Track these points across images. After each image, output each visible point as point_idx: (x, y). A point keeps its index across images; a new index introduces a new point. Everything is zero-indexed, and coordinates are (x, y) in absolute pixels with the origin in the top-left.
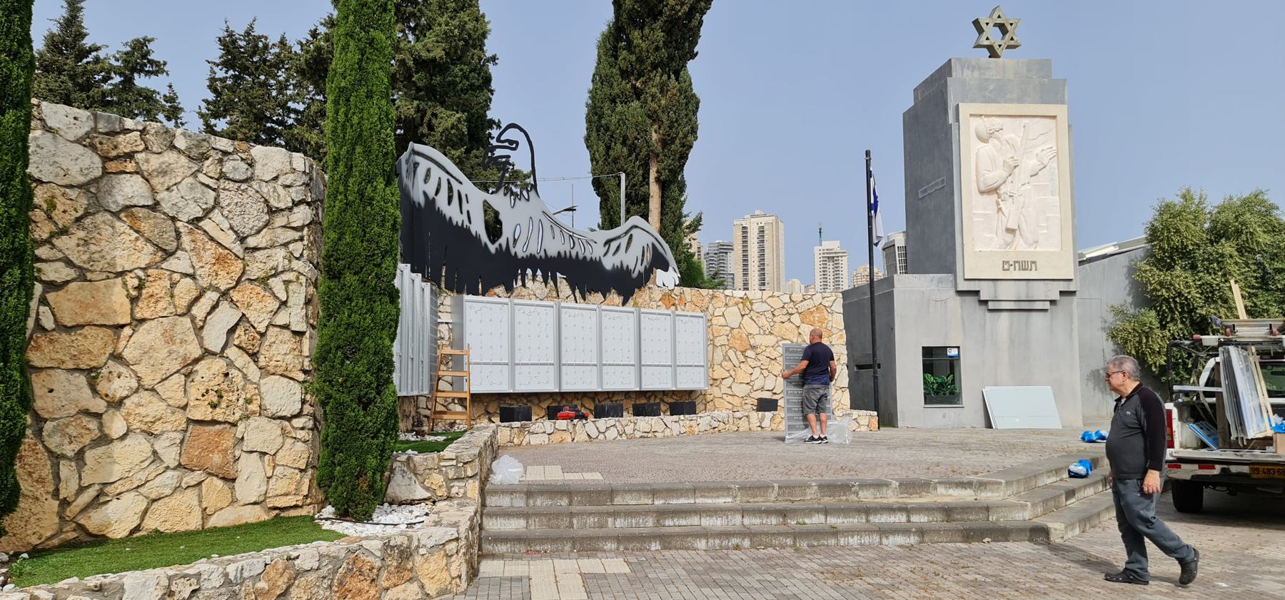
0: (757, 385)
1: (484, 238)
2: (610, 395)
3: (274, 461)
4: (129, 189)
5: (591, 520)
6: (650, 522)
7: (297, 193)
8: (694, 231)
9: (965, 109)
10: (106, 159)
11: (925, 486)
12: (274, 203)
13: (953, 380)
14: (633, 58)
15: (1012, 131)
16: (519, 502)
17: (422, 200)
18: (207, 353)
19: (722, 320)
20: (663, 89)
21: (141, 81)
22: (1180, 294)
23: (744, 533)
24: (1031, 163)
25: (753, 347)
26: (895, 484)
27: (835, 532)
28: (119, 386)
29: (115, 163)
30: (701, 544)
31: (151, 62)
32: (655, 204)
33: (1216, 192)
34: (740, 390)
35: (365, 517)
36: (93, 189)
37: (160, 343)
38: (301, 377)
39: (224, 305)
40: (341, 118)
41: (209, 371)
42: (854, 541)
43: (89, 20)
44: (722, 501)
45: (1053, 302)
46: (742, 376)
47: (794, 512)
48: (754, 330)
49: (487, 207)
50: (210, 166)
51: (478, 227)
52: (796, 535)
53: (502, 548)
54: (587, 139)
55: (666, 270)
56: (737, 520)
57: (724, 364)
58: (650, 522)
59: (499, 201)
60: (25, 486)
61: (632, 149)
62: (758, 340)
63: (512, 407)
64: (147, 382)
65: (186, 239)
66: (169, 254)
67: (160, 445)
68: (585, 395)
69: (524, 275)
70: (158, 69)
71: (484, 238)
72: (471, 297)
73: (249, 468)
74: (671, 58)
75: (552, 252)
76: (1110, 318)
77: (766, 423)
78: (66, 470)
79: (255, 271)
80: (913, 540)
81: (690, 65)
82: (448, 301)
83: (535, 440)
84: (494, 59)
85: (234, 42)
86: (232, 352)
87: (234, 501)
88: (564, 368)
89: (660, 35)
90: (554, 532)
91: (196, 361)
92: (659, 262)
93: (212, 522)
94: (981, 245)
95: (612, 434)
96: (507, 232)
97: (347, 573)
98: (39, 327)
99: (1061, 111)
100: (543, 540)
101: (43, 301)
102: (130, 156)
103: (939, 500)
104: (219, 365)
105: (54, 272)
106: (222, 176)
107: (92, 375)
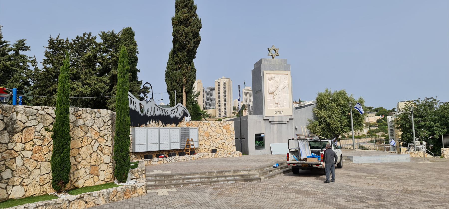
1: (140, 112)
2: (172, 150)
3: (106, 172)
4: (80, 122)
6: (181, 181)
7: (109, 118)
9: (265, 72)
10: (76, 117)
11: (238, 171)
12: (105, 121)
13: (263, 143)
15: (277, 78)
16: (153, 178)
20: (187, 67)
21: (21, 53)
22: (323, 117)
23: (200, 183)
24: (282, 86)
25: (211, 136)
27: (218, 181)
28: (80, 159)
29: (78, 117)
30: (192, 185)
31: (25, 47)
33: (334, 89)
34: (207, 147)
35: (125, 182)
38: (110, 155)
39: (97, 142)
40: (119, 105)
41: (94, 155)
42: (222, 183)
45: (287, 121)
46: (208, 143)
47: (211, 178)
48: (211, 131)
49: (140, 104)
51: (138, 110)
52: (211, 182)
53: (151, 188)
54: (166, 80)
55: (187, 116)
56: (199, 180)
58: (181, 181)
61: (178, 83)
62: (212, 134)
63: (148, 155)
64: (84, 158)
65: (90, 130)
66: (87, 133)
68: (166, 151)
70: (27, 49)
71: (140, 112)
73: (102, 173)
74: (189, 59)
75: (157, 114)
76: (308, 122)
77: (213, 156)
79: (102, 135)
80: (234, 182)
81: (194, 60)
83: (154, 163)
84: (138, 52)
87: (99, 180)
89: (185, 54)
92: (185, 115)
93: (95, 184)
94: (269, 107)
95: (173, 161)
96: (146, 110)
97: (126, 192)
99: (289, 72)
102: (80, 115)
104: (96, 154)
106: (96, 117)
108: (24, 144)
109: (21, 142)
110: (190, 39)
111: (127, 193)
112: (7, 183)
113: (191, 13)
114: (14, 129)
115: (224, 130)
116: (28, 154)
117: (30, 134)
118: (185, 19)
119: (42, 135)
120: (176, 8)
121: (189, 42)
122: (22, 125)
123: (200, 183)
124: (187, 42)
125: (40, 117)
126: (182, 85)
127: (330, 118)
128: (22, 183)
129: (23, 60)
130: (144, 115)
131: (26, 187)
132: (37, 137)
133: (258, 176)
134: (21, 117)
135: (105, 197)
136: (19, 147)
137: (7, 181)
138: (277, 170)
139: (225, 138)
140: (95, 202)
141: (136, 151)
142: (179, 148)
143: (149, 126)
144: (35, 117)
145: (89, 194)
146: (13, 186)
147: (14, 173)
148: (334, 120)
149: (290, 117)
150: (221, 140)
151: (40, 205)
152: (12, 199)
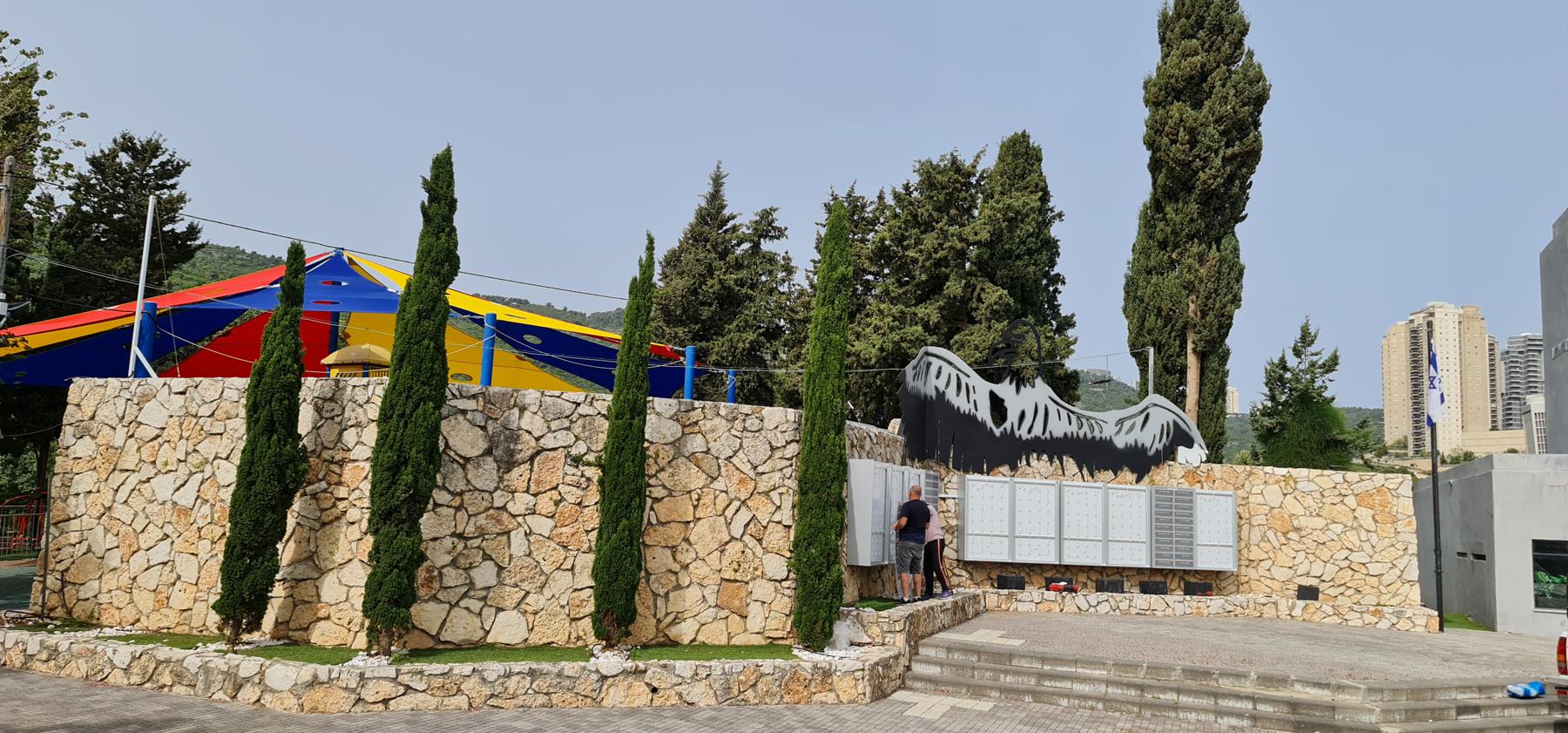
0: (1302, 569)
1: (990, 424)
3: (770, 608)
4: (696, 444)
5: (988, 674)
6: (1033, 681)
7: (789, 436)
8: (1327, 372)
10: (684, 426)
11: (1283, 681)
14: (1169, 230)
16: (942, 655)
17: (934, 394)
19: (1260, 499)
20: (1201, 259)
21: (766, 246)
23: (1097, 699)
25: (1297, 529)
26: (1253, 675)
27: (1175, 707)
28: (686, 557)
29: (689, 427)
30: (1064, 702)
34: (1281, 574)
35: (820, 649)
36: (677, 444)
39: (743, 509)
41: (734, 549)
42: (1192, 716)
43: (728, 193)
44: (1097, 673)
46: (1283, 558)
47: (1150, 688)
48: (1299, 510)
50: (738, 424)
51: (984, 414)
52: (1142, 705)
53: (919, 685)
54: (1125, 310)
56: (1102, 688)
57: (1262, 544)
58: (1033, 681)
59: (1005, 390)
60: (640, 610)
61: (1168, 320)
62: (1302, 522)
63: (1010, 576)
64: (701, 555)
67: (707, 592)
68: (1092, 568)
70: (780, 233)
71: (990, 424)
72: (977, 476)
73: (755, 610)
74: (1209, 227)
77: (1297, 612)
78: (660, 602)
79: (761, 488)
80: (1246, 723)
81: (1239, 228)
82: (955, 479)
83: (1022, 607)
86: (747, 538)
88: (1066, 543)
89: (1194, 208)
90: (961, 680)
96: (1012, 417)
97: (788, 681)
98: (650, 523)
100: (947, 683)
101: (652, 509)
102: (696, 423)
103: (1296, 696)
104: (738, 546)
105: (658, 492)
106: (745, 429)
107: (674, 549)
108: (535, 495)
109: (527, 491)
110: (1209, 148)
111: (794, 686)
112: (484, 599)
113: (1219, 49)
114: (511, 453)
115: (1364, 514)
116: (542, 525)
117: (552, 470)
118: (1192, 77)
120: (1162, 40)
121: (1204, 159)
122: (533, 443)
123: (1097, 699)
124: (1198, 163)
125: (580, 422)
126: (1185, 327)
128: (523, 606)
129: (769, 267)
130: (1004, 433)
131: (531, 618)
132: (568, 479)
133: (1374, 719)
134: (531, 422)
135: (716, 686)
136: (520, 503)
137: (484, 593)
138: (1523, 711)
139: (1367, 546)
140: (680, 695)
141: (970, 557)
142: (1144, 563)
143: (1025, 475)
144: (567, 424)
145: (665, 666)
146: (500, 610)
147: (505, 574)
150: (1345, 553)
151: (517, 670)
152: (492, 646)
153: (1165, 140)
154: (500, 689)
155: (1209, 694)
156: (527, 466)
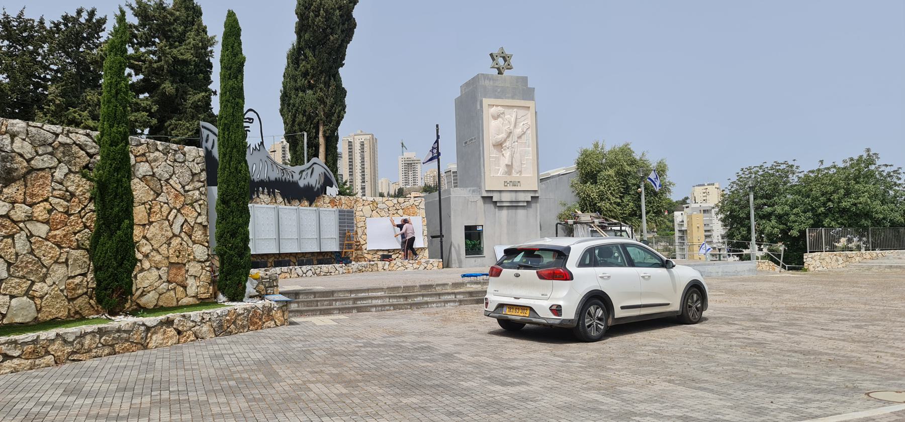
2: (304, 254)
6: (351, 302)
9: (486, 102)
12: (194, 171)
13: (480, 243)
18: (174, 235)
22: (589, 196)
24: (518, 131)
32: (322, 150)
33: (610, 143)
37: (158, 232)
40: (226, 136)
41: (175, 242)
44: (379, 294)
45: (527, 202)
54: (281, 111)
55: (332, 187)
65: (164, 188)
66: (158, 195)
69: (258, 191)
73: (191, 282)
77: (386, 267)
81: (341, 70)
85: (9, 22)
87: (187, 295)
91: (171, 238)
106: (175, 161)
108: (30, 206)
109: (24, 203)
116: (41, 230)
119: (67, 191)
121: (332, 29)
122: (25, 164)
127: (602, 200)
131: (38, 301)
144: (50, 149)
148: (611, 204)
149: (533, 195)
151: (89, 330)
153: (311, 14)
154: (78, 346)
155: (436, 294)
156: (22, 182)
